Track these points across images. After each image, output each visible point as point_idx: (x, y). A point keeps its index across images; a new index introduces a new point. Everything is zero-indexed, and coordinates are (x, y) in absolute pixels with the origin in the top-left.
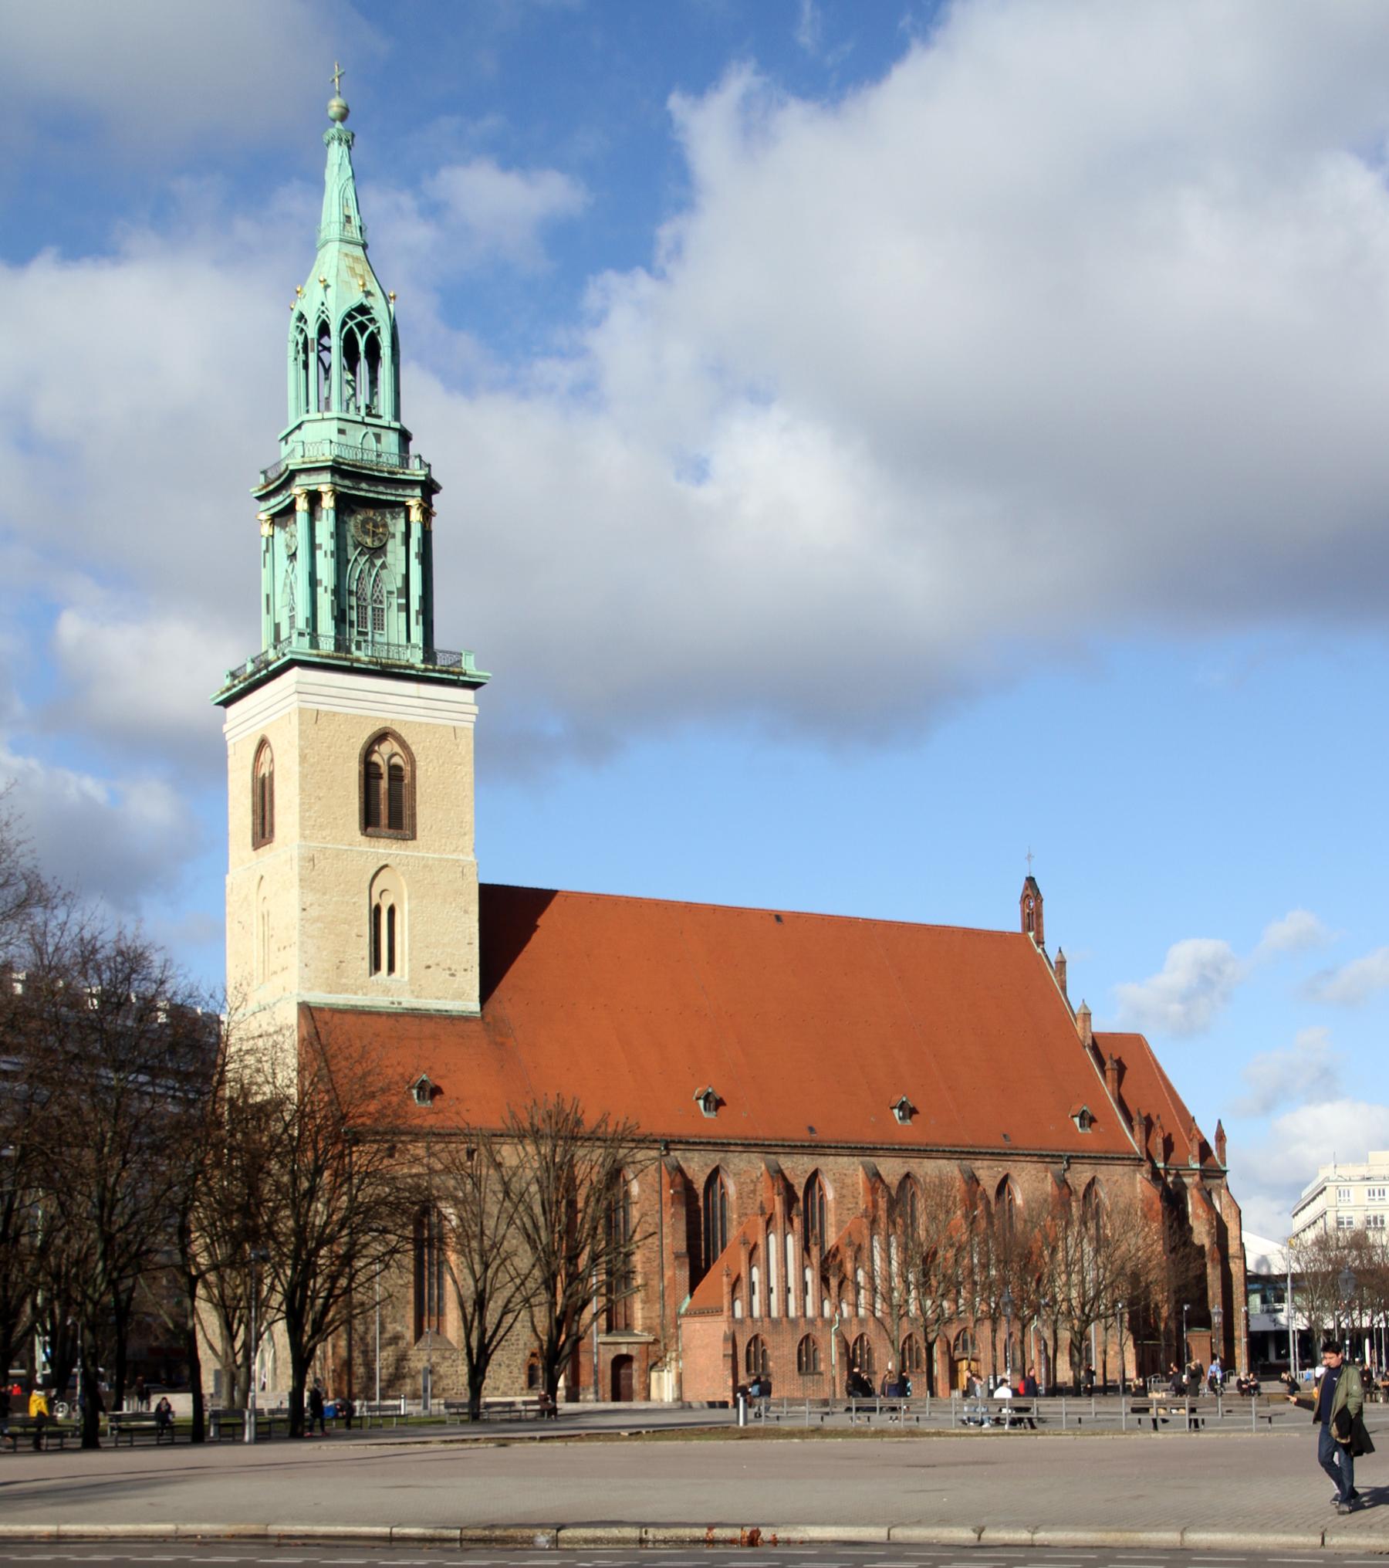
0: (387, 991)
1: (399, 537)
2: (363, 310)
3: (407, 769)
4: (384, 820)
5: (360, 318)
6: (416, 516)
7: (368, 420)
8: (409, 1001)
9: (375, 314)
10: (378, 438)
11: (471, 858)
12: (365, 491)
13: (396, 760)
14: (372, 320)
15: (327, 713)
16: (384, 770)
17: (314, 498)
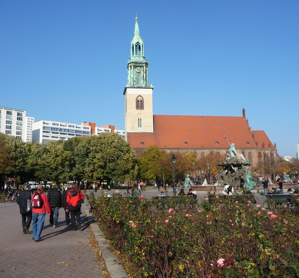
0: (140, 130)
1: (143, 70)
2: (138, 42)
3: (143, 101)
4: (140, 107)
5: (138, 43)
6: (145, 67)
7: (138, 56)
8: (143, 131)
9: (140, 42)
10: (140, 58)
11: (152, 111)
12: (137, 65)
13: (141, 99)
14: (139, 44)
15: (131, 94)
16: (140, 101)
17: (131, 67)
